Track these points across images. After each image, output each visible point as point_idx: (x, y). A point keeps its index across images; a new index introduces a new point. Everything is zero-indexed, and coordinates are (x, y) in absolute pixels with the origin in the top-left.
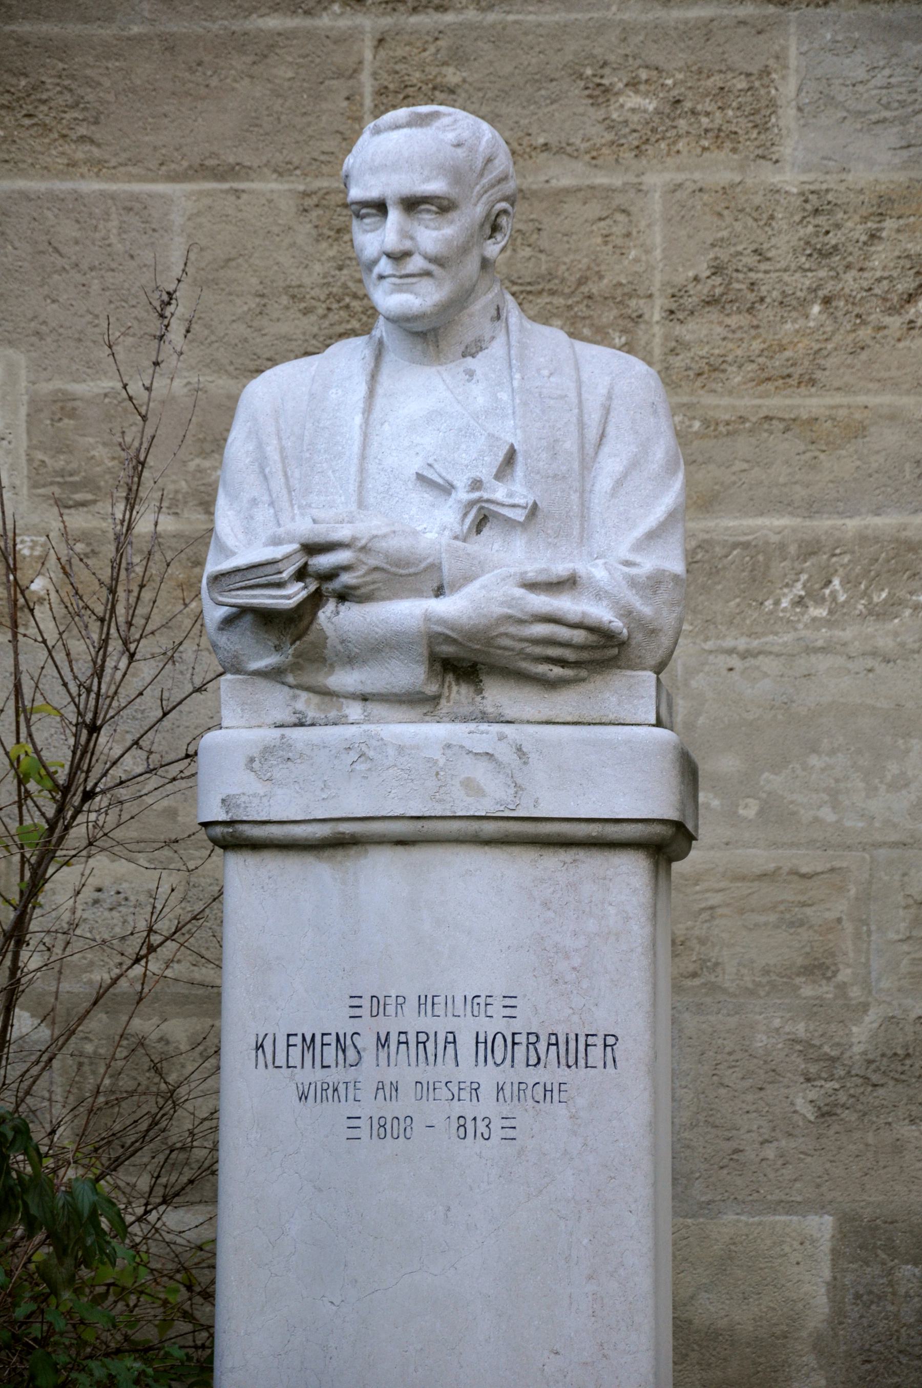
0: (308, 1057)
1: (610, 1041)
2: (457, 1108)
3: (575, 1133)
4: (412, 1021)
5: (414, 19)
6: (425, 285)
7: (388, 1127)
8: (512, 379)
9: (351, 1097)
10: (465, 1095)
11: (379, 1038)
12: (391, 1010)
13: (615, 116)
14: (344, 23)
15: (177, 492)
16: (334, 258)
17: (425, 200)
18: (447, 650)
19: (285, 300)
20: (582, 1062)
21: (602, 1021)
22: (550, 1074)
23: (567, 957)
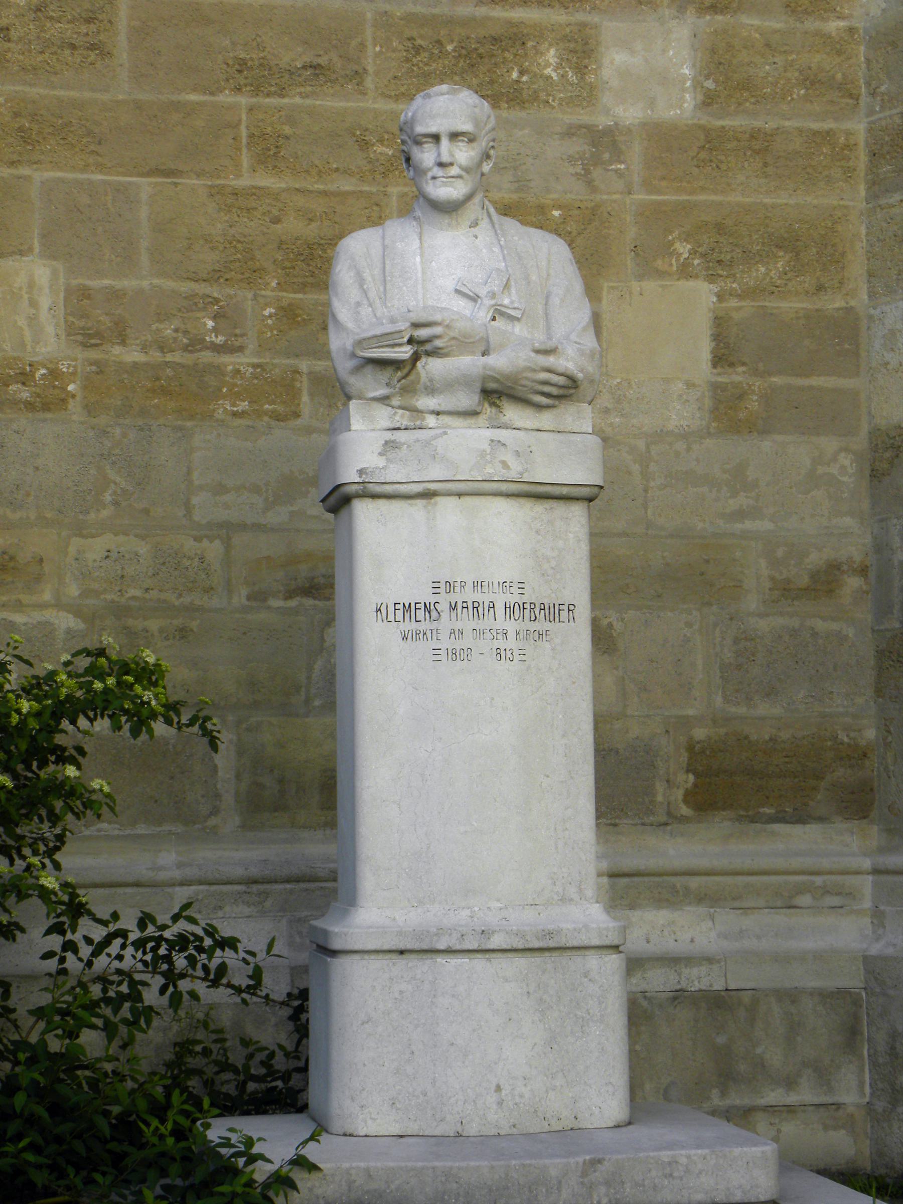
0: (407, 615)
1: (571, 607)
2: (496, 644)
3: (554, 658)
4: (470, 596)
5: (267, 100)
6: (459, 181)
7: (458, 654)
8: (499, 241)
9: (435, 638)
10: (499, 636)
11: (451, 605)
12: (457, 589)
13: (372, 156)
14: (231, 100)
15: (146, 340)
16: (227, 221)
17: (463, 134)
18: (492, 385)
19: (201, 242)
20: (557, 619)
21: (567, 597)
22: (542, 625)
23: (549, 562)
